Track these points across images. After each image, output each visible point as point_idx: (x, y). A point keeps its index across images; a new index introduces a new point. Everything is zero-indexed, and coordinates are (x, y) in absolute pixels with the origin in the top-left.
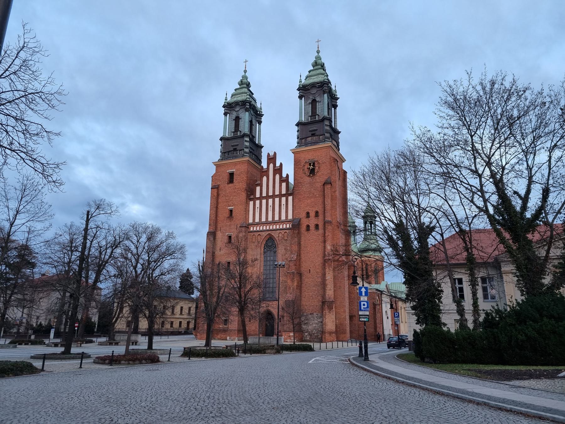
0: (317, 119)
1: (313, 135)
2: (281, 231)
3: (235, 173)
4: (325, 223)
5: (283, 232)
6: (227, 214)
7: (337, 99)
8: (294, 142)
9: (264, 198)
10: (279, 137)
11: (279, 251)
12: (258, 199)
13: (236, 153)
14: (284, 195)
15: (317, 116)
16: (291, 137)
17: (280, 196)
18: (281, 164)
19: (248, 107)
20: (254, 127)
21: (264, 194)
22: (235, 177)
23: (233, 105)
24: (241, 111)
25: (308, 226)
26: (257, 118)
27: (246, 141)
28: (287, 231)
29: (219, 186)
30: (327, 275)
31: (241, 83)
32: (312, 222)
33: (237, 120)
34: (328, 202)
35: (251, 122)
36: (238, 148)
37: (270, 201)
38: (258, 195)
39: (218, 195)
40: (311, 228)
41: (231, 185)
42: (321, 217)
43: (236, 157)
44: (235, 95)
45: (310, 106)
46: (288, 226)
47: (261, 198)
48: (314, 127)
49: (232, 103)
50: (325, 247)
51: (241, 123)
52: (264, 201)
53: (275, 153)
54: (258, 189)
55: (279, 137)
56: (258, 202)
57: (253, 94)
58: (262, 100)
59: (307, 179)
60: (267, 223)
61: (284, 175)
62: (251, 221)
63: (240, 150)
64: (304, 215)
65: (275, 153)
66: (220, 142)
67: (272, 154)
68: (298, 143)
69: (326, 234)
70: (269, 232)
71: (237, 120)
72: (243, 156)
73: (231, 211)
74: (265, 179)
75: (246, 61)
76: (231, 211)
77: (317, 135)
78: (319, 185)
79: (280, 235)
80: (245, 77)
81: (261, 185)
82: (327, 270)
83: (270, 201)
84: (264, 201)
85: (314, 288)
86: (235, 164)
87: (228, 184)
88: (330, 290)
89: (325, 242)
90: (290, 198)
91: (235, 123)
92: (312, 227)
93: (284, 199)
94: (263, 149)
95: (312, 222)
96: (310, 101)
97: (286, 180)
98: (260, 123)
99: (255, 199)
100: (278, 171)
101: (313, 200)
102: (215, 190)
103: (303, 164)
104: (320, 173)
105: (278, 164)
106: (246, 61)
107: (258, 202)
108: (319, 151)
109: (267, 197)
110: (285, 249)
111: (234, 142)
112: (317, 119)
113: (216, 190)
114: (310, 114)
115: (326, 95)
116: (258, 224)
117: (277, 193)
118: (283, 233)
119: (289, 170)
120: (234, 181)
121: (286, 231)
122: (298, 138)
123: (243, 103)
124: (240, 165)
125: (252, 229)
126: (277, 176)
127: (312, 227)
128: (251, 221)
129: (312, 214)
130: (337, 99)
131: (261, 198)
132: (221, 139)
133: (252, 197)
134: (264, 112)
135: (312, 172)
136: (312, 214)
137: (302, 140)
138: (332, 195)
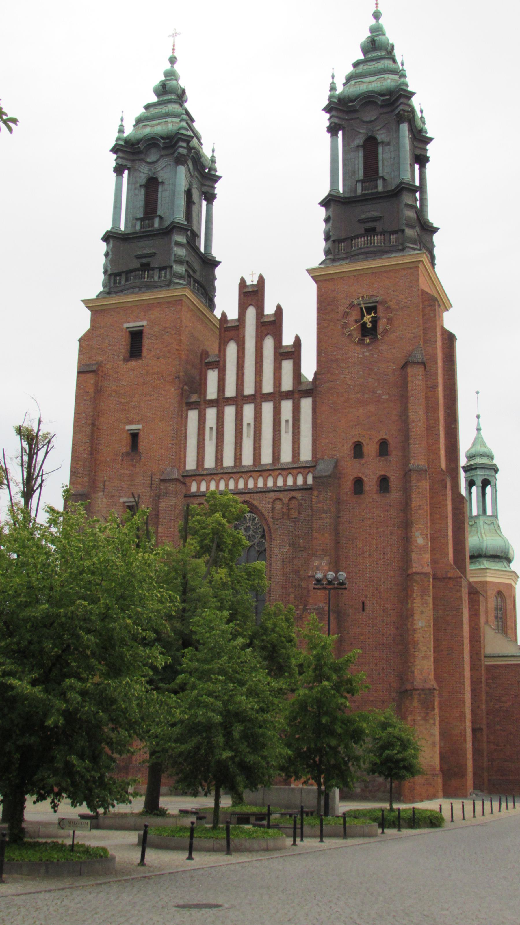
0: (380, 189)
1: (370, 231)
2: (281, 495)
3: (146, 331)
4: (406, 474)
5: (285, 497)
6: (124, 446)
7: (429, 140)
8: (315, 252)
9: (230, 401)
11: (276, 550)
12: (212, 403)
13: (150, 277)
14: (288, 395)
15: (380, 183)
16: (309, 239)
17: (278, 396)
18: (279, 310)
19: (184, 151)
20: (195, 208)
21: (230, 391)
22: (146, 342)
23: (141, 146)
24: (162, 163)
26: (203, 185)
27: (178, 244)
28: (298, 495)
29: (100, 365)
30: (416, 617)
32: (371, 470)
33: (151, 186)
34: (417, 413)
35: (189, 193)
36: (155, 263)
37: (248, 410)
38: (212, 393)
39: (99, 391)
40: (366, 488)
41: (133, 363)
42: (395, 455)
43: (150, 287)
45: (361, 154)
46: (300, 481)
47: (220, 402)
49: (139, 141)
50: (407, 540)
51: (163, 195)
52: (230, 412)
53: (261, 279)
54: (212, 376)
56: (211, 414)
57: (192, 120)
59: (356, 352)
60: (238, 471)
61: (287, 340)
62: (191, 464)
63: (161, 269)
64: (347, 449)
65: (261, 279)
66: (103, 247)
67: (251, 280)
68: (327, 252)
69: (414, 504)
70: (247, 497)
71: (151, 186)
72: (169, 284)
73: (135, 436)
74: (232, 349)
75: (175, 35)
76: (135, 436)
77: (383, 233)
79: (279, 505)
80: (171, 75)
81: (220, 365)
82: (417, 602)
83: (248, 410)
84: (230, 412)
85: (376, 654)
86: (149, 306)
87: (126, 360)
88: (426, 657)
89: (406, 525)
90: (306, 404)
91: (147, 195)
92: (371, 484)
93: (287, 406)
94: (218, 271)
95: (371, 470)
96: (359, 141)
97: (294, 353)
98: (210, 198)
99: (202, 405)
100: (272, 326)
101: (372, 408)
102: (91, 379)
103: (343, 309)
104: (392, 336)
105: (269, 310)
106: (175, 35)
107: (211, 414)
109: (240, 400)
110: (292, 545)
111: (145, 247)
112: (380, 189)
113: (90, 376)
114: (361, 175)
115: (404, 127)
116: (212, 475)
117: (268, 387)
118: (286, 500)
119: (301, 324)
120: (145, 353)
121: (293, 494)
122: (327, 239)
125: (194, 488)
126: (269, 343)
127: (371, 484)
128: (191, 464)
129: (371, 449)
130: (429, 140)
131: (220, 402)
132: (107, 238)
133: (194, 398)
134: (220, 170)
135: (369, 332)
136: (371, 449)
137: (338, 244)
138: (427, 398)
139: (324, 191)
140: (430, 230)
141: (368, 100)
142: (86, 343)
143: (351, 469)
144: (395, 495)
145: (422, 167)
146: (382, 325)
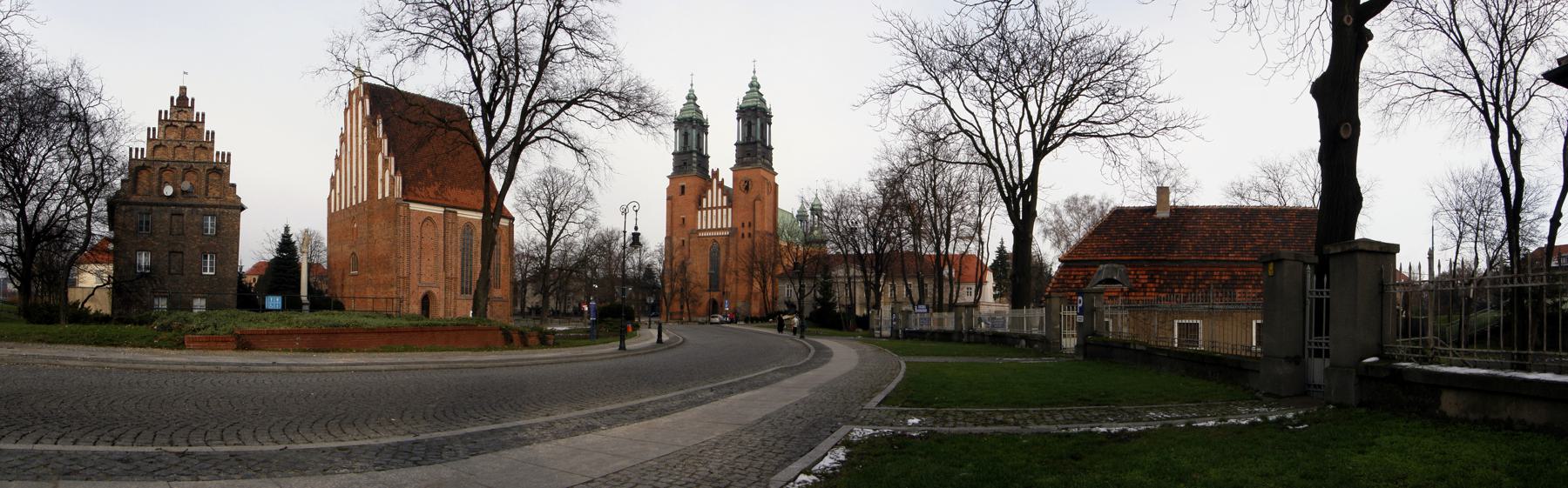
8: (733, 163)
10: (722, 153)
31: (688, 98)
33: (685, 136)
34: (758, 216)
55: (722, 153)
58: (708, 113)
60: (712, 230)
95: (746, 231)
100: (721, 185)
108: (749, 173)
119: (729, 183)
124: (691, 182)
135: (747, 188)
140: (770, 148)
142: (669, 189)
143: (741, 230)
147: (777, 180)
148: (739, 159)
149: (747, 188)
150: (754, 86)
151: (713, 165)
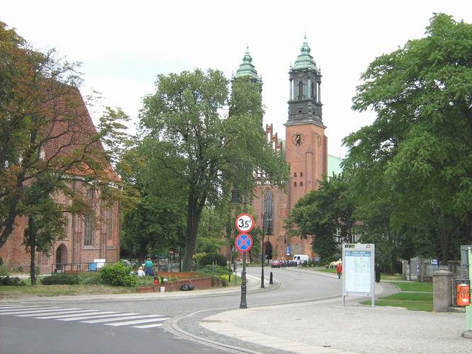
8: (285, 117)
25: (295, 183)
42: (304, 177)
44: (240, 71)
48: (300, 106)
58: (262, 72)
59: (295, 148)
67: (269, 125)
78: (304, 153)
105: (274, 134)
108: (305, 130)
114: (298, 95)
123: (246, 79)
129: (298, 174)
135: (299, 142)
136: (298, 174)
139: (288, 100)
141: (300, 70)
144: (304, 187)
145: (319, 85)
146: (301, 140)
147: (327, 133)
148: (291, 115)
149: (299, 142)
150: (306, 51)
151: (266, 121)
